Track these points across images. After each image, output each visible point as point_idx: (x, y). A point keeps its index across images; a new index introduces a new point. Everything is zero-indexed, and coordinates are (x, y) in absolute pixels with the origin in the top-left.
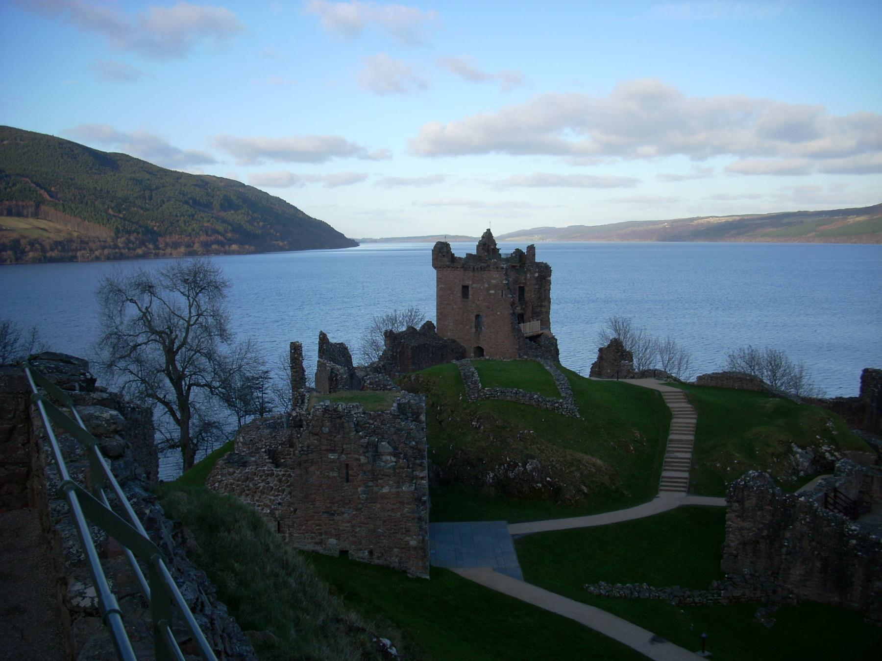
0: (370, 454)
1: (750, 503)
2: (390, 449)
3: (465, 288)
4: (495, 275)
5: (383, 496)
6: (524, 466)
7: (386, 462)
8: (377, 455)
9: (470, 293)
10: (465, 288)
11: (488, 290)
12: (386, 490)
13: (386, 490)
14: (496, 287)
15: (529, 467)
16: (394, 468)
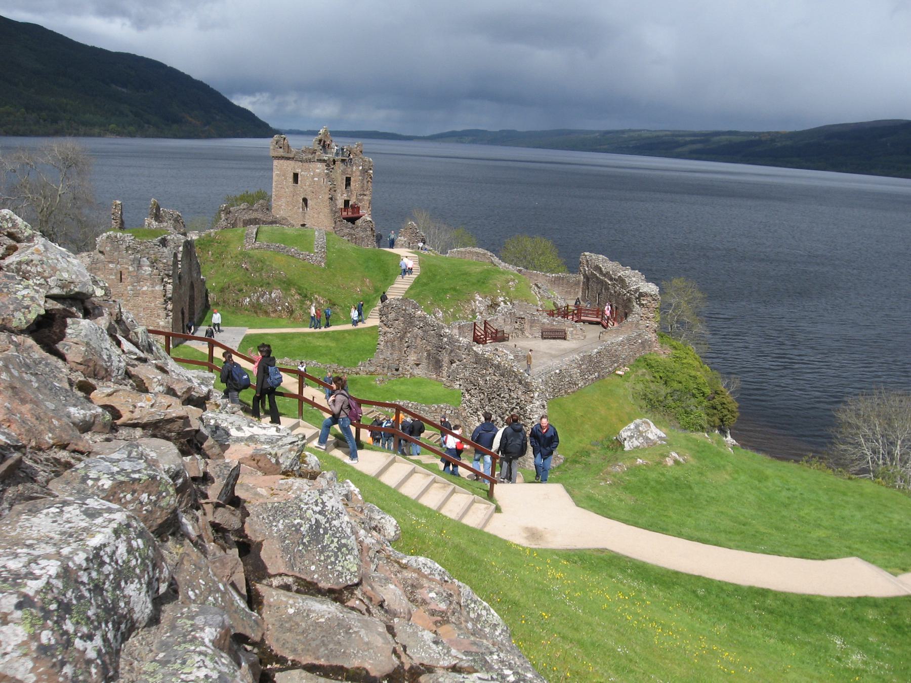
0: (135, 265)
1: (392, 316)
2: (148, 263)
3: (296, 176)
4: (319, 165)
5: (144, 293)
6: (270, 295)
7: (145, 271)
8: (140, 266)
9: (299, 179)
10: (296, 176)
11: (313, 177)
12: (145, 288)
13: (145, 288)
14: (319, 175)
15: (273, 295)
16: (150, 275)
